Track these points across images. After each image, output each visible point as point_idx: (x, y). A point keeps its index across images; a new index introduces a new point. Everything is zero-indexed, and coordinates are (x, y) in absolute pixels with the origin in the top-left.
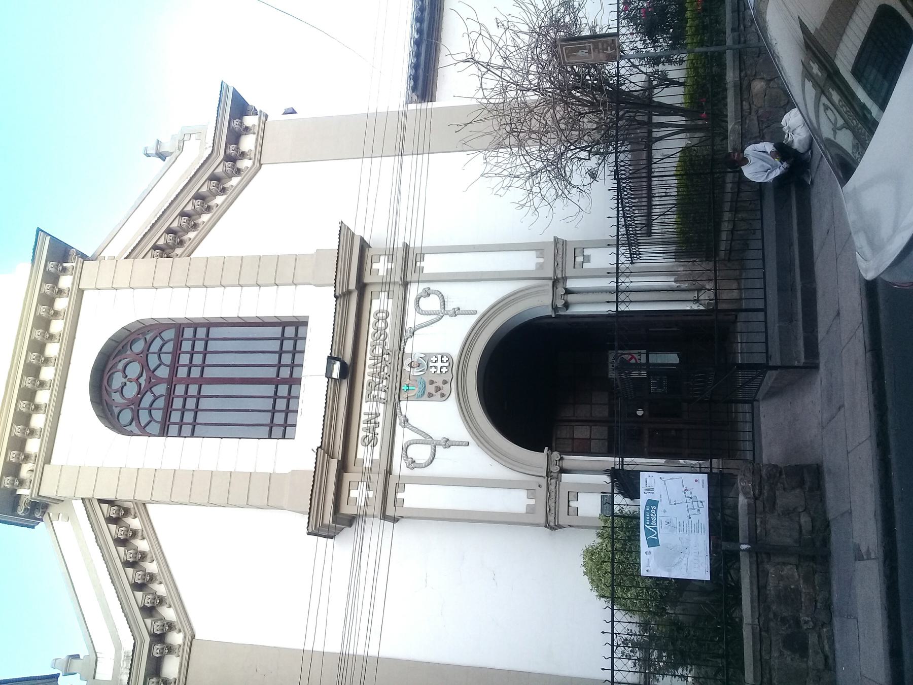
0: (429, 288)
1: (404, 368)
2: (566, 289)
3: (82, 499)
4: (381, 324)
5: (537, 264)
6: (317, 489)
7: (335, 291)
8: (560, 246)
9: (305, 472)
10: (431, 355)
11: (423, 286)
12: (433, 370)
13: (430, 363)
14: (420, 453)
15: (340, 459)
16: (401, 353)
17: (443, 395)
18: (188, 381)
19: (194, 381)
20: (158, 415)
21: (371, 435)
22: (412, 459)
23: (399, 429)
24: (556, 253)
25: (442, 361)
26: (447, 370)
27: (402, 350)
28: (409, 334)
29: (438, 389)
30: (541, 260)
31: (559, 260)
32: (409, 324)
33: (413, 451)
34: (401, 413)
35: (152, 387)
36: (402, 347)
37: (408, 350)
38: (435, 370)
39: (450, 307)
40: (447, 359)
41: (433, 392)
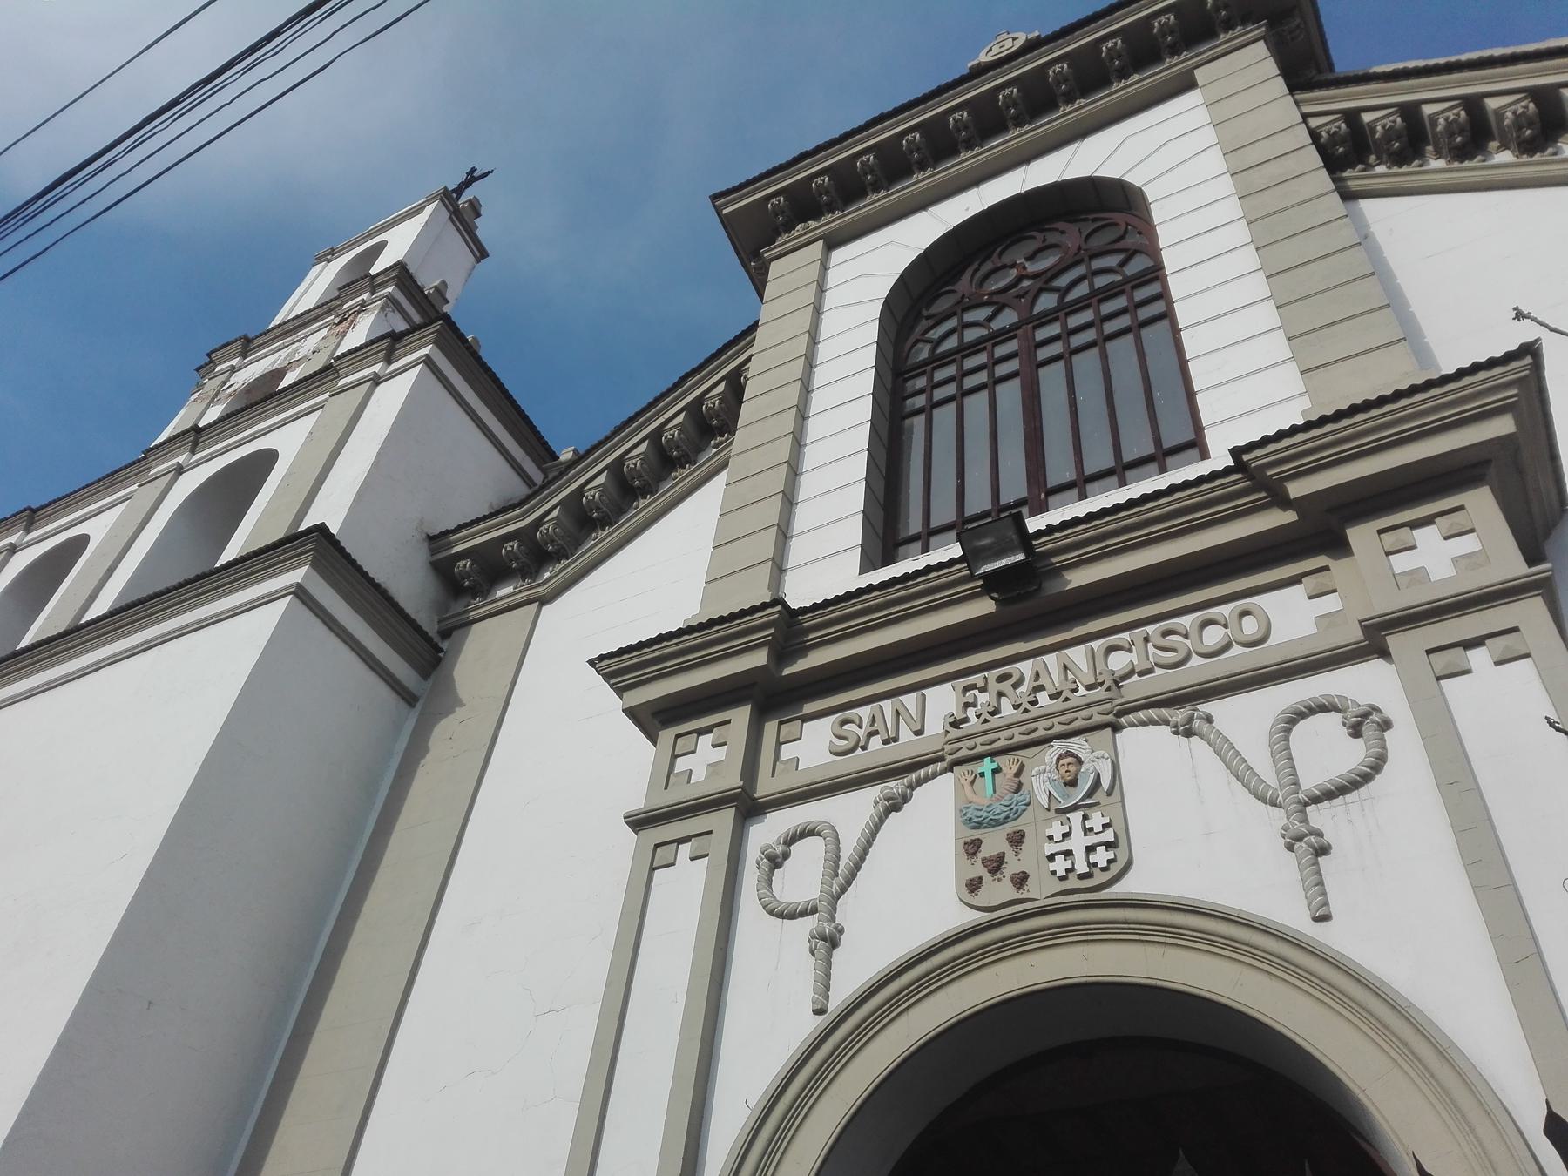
0: (1386, 725)
1: (1056, 743)
4: (1213, 636)
6: (687, 641)
7: (1251, 446)
12: (1057, 830)
13: (1080, 814)
15: (787, 671)
16: (1110, 718)
17: (974, 886)
22: (786, 856)
25: (1090, 849)
26: (1061, 873)
27: (1122, 720)
28: (1179, 720)
29: (996, 865)
34: (920, 782)
35: (1009, 306)
36: (1131, 717)
38: (1058, 837)
41: (987, 851)
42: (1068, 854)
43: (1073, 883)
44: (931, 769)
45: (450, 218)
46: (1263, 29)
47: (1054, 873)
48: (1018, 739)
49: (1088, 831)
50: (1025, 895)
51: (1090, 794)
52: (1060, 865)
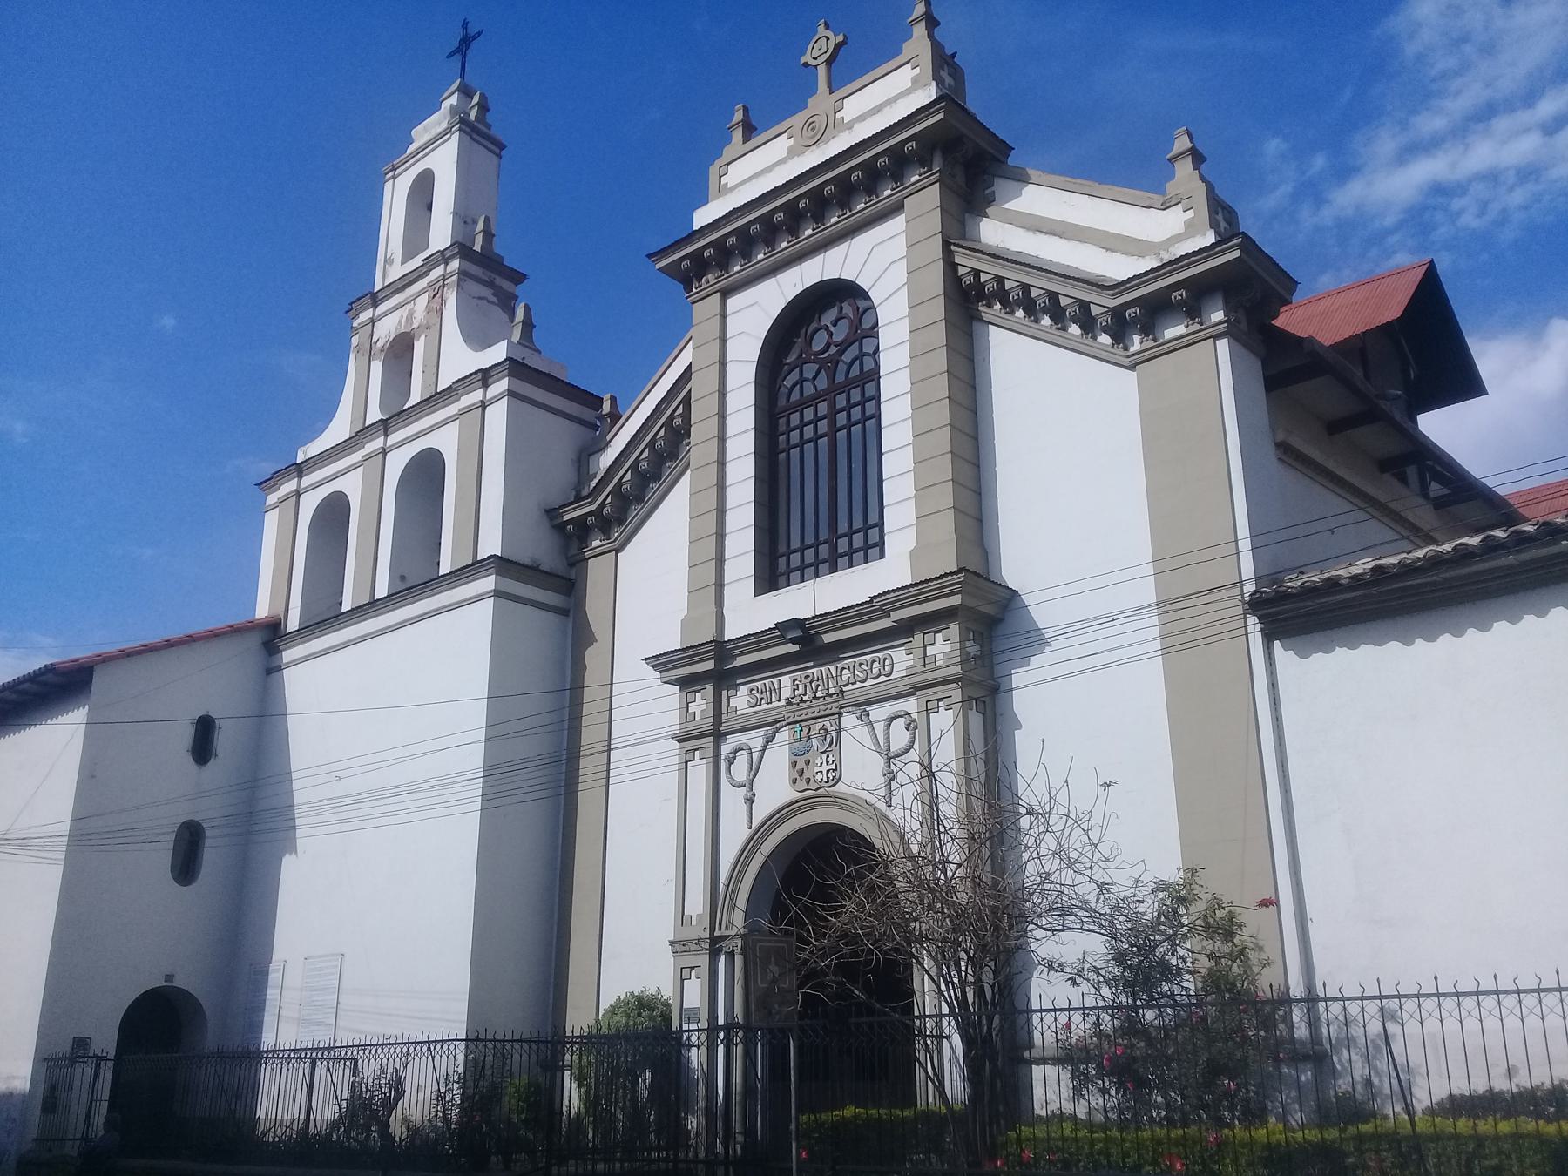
0: (916, 728)
12: (819, 761)
14: (740, 770)
17: (794, 782)
18: (833, 412)
19: (832, 423)
20: (795, 396)
21: (757, 695)
22: (734, 758)
23: (761, 732)
25: (828, 771)
29: (801, 773)
34: (775, 732)
41: (799, 766)
42: (821, 772)
43: (823, 784)
45: (471, 138)
46: (938, 175)
48: (810, 716)
49: (827, 763)
51: (829, 746)
52: (819, 777)
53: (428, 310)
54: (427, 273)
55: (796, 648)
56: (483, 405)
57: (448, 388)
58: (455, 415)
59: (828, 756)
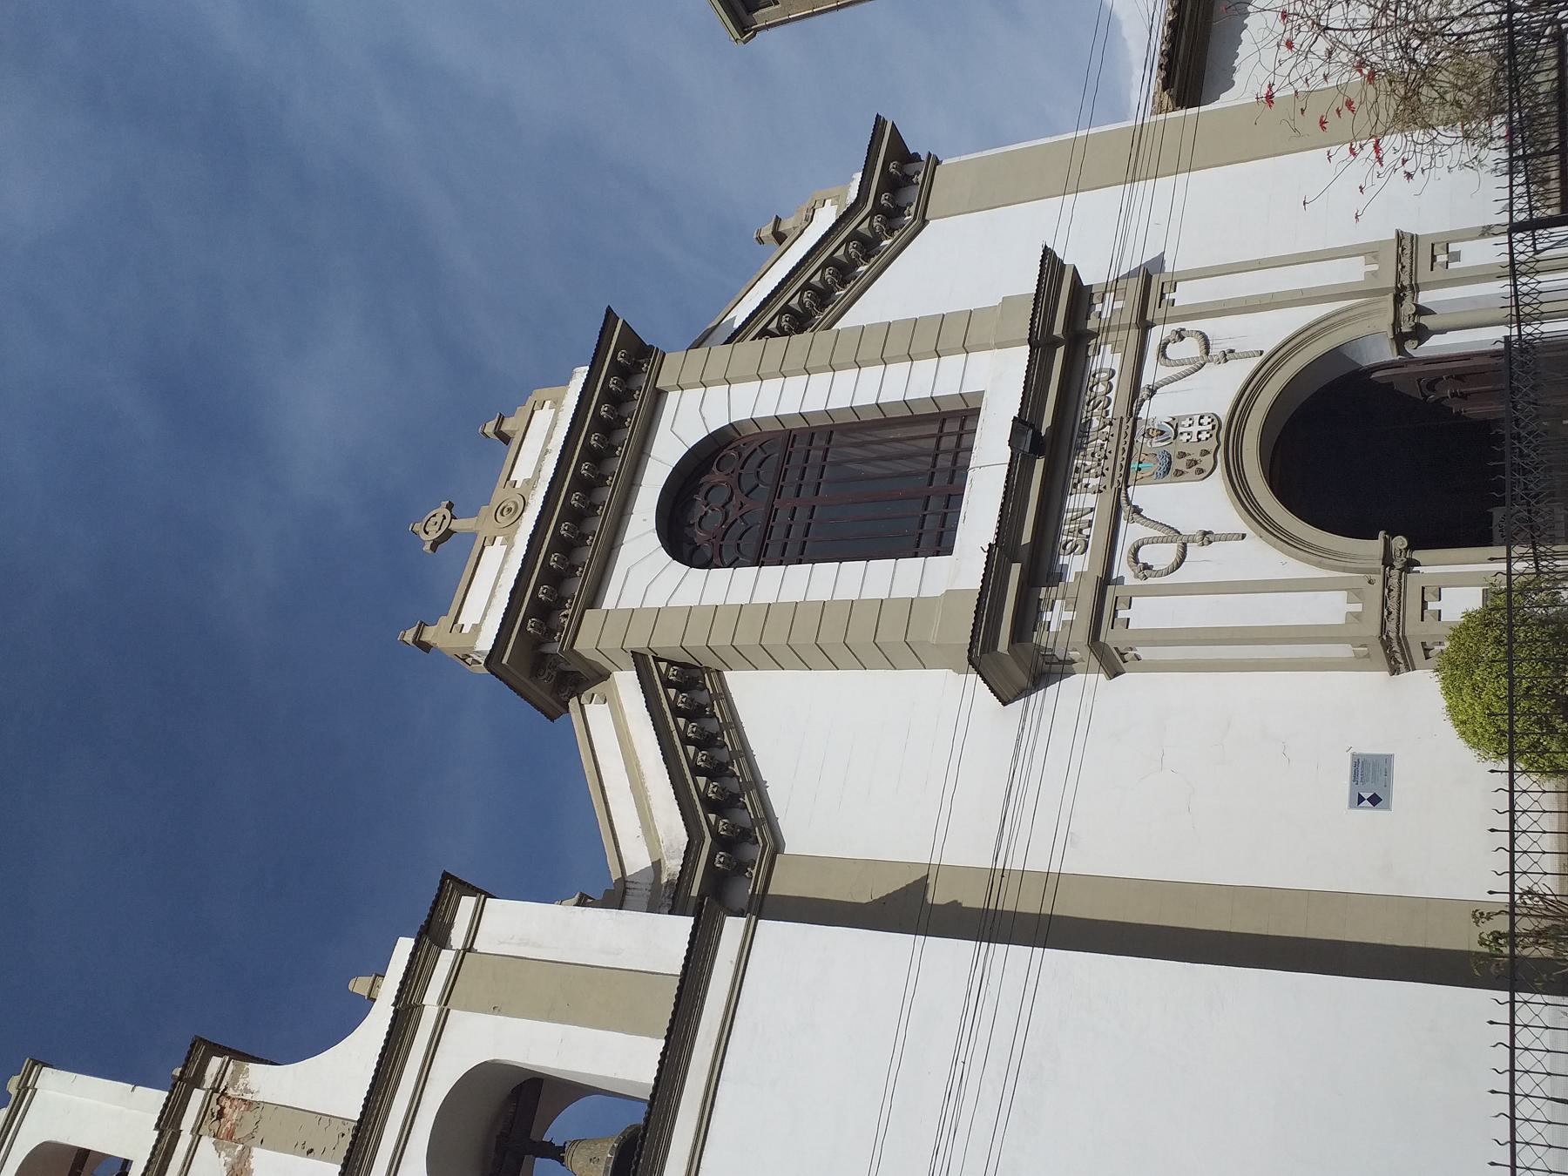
2: (1417, 306)
3: (634, 654)
5: (1366, 273)
8: (1407, 243)
9: (965, 593)
10: (1184, 418)
11: (1170, 328)
14: (1160, 555)
16: (1132, 419)
17: (1201, 471)
23: (1123, 523)
24: (1400, 252)
25: (1200, 424)
26: (1208, 435)
30: (1375, 267)
31: (1406, 261)
32: (1147, 380)
33: (1143, 556)
37: (1142, 414)
38: (1189, 437)
39: (1215, 350)
40: (1210, 420)
42: (1199, 433)
44: (1123, 495)
47: (1207, 439)
49: (1190, 425)
50: (1213, 451)
51: (1172, 426)
53: (225, 1138)
54: (177, 1135)
55: (1040, 464)
56: (468, 949)
57: (394, 1020)
58: (441, 1011)
59: (1183, 426)
